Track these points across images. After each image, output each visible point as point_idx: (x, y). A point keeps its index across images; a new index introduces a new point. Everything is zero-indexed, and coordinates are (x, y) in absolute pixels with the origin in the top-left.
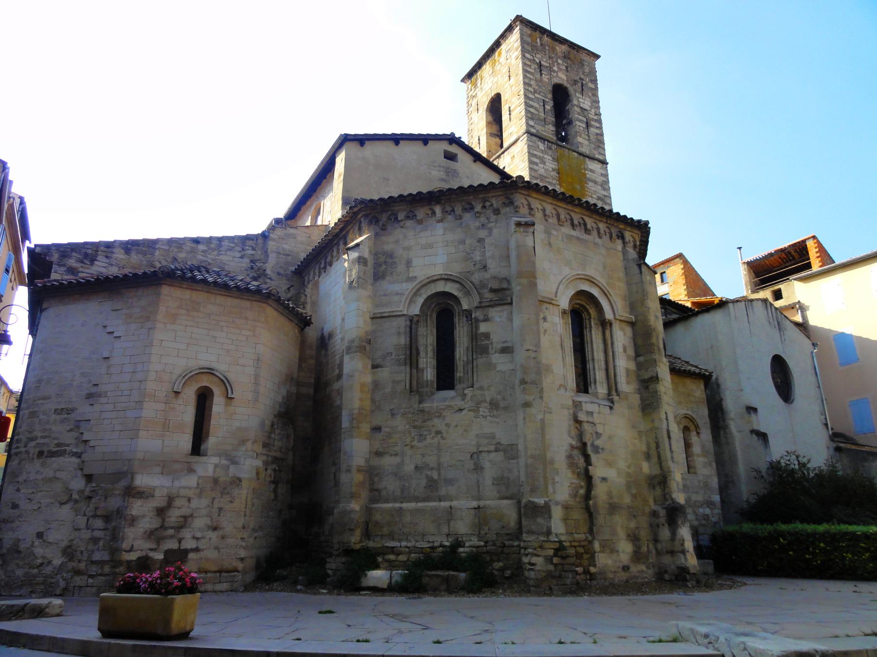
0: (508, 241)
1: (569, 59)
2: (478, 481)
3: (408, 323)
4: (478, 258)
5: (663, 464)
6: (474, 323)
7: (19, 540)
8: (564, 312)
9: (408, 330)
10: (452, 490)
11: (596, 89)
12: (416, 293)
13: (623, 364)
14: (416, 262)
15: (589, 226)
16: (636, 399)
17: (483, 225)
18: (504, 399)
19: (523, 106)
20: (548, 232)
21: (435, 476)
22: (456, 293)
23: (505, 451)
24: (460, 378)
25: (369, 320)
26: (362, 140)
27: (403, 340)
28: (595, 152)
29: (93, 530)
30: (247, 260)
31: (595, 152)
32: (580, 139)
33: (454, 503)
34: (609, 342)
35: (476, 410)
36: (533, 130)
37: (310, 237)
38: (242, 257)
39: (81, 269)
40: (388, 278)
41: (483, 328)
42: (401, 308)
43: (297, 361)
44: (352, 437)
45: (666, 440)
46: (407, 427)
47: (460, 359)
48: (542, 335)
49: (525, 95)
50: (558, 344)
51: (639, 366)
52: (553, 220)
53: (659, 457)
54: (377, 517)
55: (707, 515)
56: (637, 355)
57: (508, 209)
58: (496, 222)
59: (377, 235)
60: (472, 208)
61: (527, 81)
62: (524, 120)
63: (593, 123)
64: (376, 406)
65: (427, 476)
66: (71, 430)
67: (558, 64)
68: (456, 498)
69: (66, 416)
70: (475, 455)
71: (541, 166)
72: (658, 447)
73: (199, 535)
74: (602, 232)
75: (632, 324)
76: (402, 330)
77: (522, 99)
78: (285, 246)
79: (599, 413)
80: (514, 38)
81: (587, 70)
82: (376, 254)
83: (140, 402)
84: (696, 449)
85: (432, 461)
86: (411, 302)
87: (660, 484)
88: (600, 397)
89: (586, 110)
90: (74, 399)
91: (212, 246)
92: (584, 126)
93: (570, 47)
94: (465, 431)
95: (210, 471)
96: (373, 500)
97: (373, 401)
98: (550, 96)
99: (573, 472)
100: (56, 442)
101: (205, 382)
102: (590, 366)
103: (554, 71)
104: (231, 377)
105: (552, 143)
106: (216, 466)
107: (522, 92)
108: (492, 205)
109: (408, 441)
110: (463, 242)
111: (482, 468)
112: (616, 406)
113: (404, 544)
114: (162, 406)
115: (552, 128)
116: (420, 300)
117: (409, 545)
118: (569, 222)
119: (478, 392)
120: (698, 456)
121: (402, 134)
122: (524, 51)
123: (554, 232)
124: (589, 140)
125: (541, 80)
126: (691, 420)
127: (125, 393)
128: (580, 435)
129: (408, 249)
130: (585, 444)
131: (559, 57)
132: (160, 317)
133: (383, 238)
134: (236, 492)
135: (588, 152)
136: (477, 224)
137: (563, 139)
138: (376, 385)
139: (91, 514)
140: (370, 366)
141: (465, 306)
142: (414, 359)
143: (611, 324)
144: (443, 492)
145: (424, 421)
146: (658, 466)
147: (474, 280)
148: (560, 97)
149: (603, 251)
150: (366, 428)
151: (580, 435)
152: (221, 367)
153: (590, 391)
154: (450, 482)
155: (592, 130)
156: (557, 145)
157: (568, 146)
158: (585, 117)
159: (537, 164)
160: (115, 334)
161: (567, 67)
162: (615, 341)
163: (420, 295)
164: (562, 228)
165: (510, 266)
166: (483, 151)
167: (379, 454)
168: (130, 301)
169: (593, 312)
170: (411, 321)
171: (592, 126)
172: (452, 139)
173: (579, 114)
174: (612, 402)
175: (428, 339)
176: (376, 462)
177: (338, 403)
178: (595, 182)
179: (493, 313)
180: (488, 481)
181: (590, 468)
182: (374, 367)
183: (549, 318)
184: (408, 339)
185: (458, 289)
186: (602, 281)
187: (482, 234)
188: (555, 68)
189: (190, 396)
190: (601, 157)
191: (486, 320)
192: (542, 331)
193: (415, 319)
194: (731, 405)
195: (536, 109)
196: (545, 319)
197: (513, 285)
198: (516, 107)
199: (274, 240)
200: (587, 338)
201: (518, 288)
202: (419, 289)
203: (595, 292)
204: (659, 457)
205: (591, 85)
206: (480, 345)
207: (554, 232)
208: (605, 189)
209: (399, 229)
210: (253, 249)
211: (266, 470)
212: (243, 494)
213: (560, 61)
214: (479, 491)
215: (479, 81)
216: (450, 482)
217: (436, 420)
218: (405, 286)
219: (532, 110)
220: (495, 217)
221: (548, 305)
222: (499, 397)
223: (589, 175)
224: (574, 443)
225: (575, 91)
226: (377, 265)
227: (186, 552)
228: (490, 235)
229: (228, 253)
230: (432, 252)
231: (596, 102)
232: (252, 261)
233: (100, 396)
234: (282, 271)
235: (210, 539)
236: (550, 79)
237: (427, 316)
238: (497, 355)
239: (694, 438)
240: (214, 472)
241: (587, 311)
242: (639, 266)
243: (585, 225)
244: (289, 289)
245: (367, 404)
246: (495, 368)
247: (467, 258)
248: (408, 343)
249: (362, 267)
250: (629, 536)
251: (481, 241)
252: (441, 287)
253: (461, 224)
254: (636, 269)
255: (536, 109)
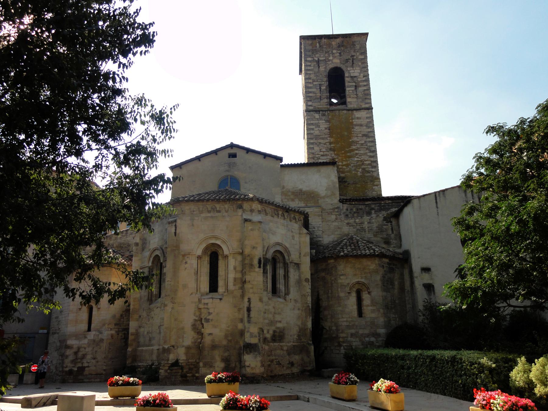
1: (343, 46)
28: (361, 104)
31: (361, 104)
81: (358, 47)
89: (355, 77)
93: (343, 37)
95: (92, 337)
106: (94, 335)
131: (335, 49)
135: (355, 106)
155: (361, 89)
158: (354, 82)
159: (313, 129)
213: (334, 51)
223: (355, 122)
225: (347, 67)
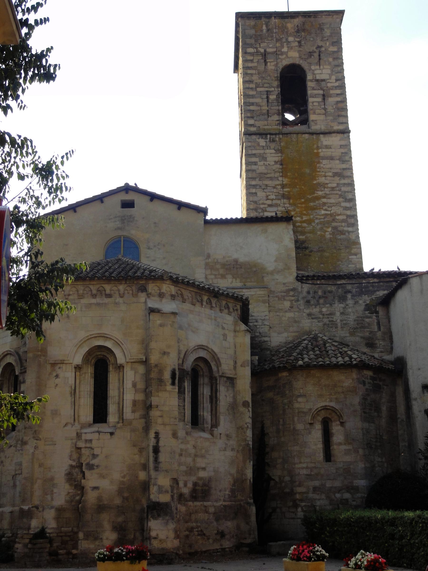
36: (253, 129)
89: (323, 80)
98: (276, 83)
125: (266, 70)
161: (299, 42)
178: (331, 158)
188: (285, 49)
223: (323, 152)
255: (257, 105)
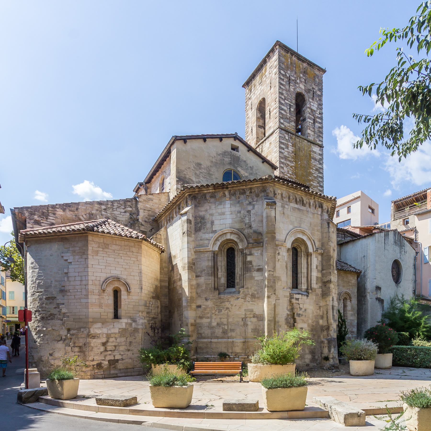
0: (262, 213)
2: (245, 331)
3: (213, 255)
4: (247, 221)
5: (329, 321)
6: (245, 256)
7: (42, 356)
8: (289, 249)
9: (213, 258)
10: (233, 334)
11: (321, 96)
12: (217, 240)
13: (315, 274)
14: (216, 222)
15: (305, 202)
16: (319, 291)
17: (250, 203)
18: (258, 294)
19: (277, 109)
20: (283, 207)
21: (226, 328)
22: (236, 240)
23: (257, 317)
24: (238, 282)
25: (193, 253)
26: (185, 139)
27: (210, 264)
29: (75, 352)
30: (128, 214)
31: (317, 140)
32: (309, 131)
33: (234, 340)
34: (310, 264)
35: (244, 298)
36: (283, 126)
37: (160, 200)
38: (125, 212)
39: (42, 221)
40: (202, 230)
41: (249, 258)
42: (210, 248)
43: (159, 270)
44: (187, 310)
45: (331, 310)
46: (213, 305)
47: (238, 273)
48: (277, 262)
49: (280, 102)
50: (285, 266)
51: (323, 275)
52: (286, 200)
53: (327, 318)
54: (200, 345)
55: (350, 337)
56: (323, 270)
57: (263, 194)
58: (257, 201)
59: (196, 206)
60: (245, 193)
61: (281, 91)
62: (278, 119)
63: (318, 120)
64: (199, 295)
65: (222, 328)
66: (55, 308)
67: (300, 78)
68: (235, 338)
69: (51, 301)
70: (244, 319)
71: (286, 150)
72: (327, 313)
73: (122, 353)
74: (312, 204)
75: (322, 254)
76: (210, 258)
77: (277, 105)
78: (147, 206)
79: (302, 299)
80: (275, 57)
82: (195, 217)
83: (87, 295)
84: (349, 308)
85: (225, 321)
86: (214, 244)
87: (326, 329)
88: (303, 290)
90: (54, 293)
91: (109, 206)
92: (312, 122)
94: (240, 308)
96: (198, 338)
97: (197, 293)
98: (294, 101)
99: (288, 326)
100: (49, 313)
101: (117, 285)
102: (299, 275)
103: (297, 83)
104: (129, 281)
105: (293, 134)
107: (277, 99)
108: (255, 191)
109: (214, 312)
110: (239, 212)
111: (247, 325)
112: (310, 295)
113: (212, 356)
114: (97, 297)
115: (293, 124)
116: (219, 243)
117: (215, 357)
118: (294, 200)
119: (246, 290)
120: (349, 311)
121: (207, 135)
122: (280, 68)
123: (286, 206)
124: (314, 132)
125: (289, 91)
126: (348, 294)
127: (79, 290)
128: (292, 309)
129: (212, 215)
130: (294, 314)
132: (90, 252)
133: (199, 208)
134: (136, 335)
136: (247, 202)
137: (298, 130)
138: (198, 285)
139: (72, 345)
140: (195, 276)
141: (240, 247)
142: (216, 273)
143: (311, 255)
144: (230, 334)
145: (221, 303)
146: (326, 322)
147: (245, 233)
148: (300, 101)
149: (310, 215)
150: (194, 306)
151: (292, 309)
152: (124, 276)
153: (299, 288)
154: (232, 330)
156: (296, 136)
157: (302, 136)
160: (69, 261)
161: (305, 81)
162: (312, 263)
163: (219, 241)
164: (291, 204)
165: (263, 226)
166: (253, 144)
167: (201, 318)
168: (73, 243)
169: (303, 248)
170: (214, 254)
171: (317, 122)
172: (236, 137)
173: (310, 114)
174: (308, 293)
175: (222, 262)
176: (198, 321)
177: (180, 292)
178: (316, 160)
179: (254, 251)
180: (250, 331)
181: (295, 324)
182: (197, 276)
183: (281, 254)
184: (213, 263)
185: (237, 238)
186: (308, 232)
187: (250, 208)
188: (298, 81)
189: (110, 290)
190: (320, 143)
191: (251, 254)
192: (277, 260)
193: (216, 253)
194: (370, 285)
195: (285, 111)
196: (279, 254)
197: (264, 237)
198: (274, 109)
199: (141, 202)
200: (299, 261)
201: (266, 239)
202: (218, 238)
203: (305, 238)
204: (327, 318)
205: (319, 93)
206: (247, 267)
207: (286, 206)
208: (320, 164)
209: (207, 203)
210: (131, 207)
211: (149, 324)
212: (140, 336)
214: (245, 334)
215: (253, 87)
216: (232, 330)
217: (226, 303)
218: (211, 235)
219: (283, 112)
220: (256, 198)
221: (281, 247)
222: (255, 292)
223: (313, 155)
224: (289, 313)
225: (309, 98)
226: (196, 224)
227: (117, 361)
228: (253, 208)
229: (118, 210)
230: (224, 217)
231: (320, 105)
232: (130, 214)
233: (66, 291)
234: (146, 220)
235: (127, 355)
236: (294, 89)
237: (222, 251)
238: (255, 272)
239: (348, 303)
240: (126, 326)
241: (300, 248)
242: (328, 223)
243: (303, 201)
244: (151, 230)
245: (194, 295)
246: (254, 279)
247: (242, 221)
248: (213, 265)
249: (189, 225)
250: (310, 352)
251: (249, 212)
252: (229, 237)
253: (239, 202)
254: (326, 225)
255: (285, 111)
